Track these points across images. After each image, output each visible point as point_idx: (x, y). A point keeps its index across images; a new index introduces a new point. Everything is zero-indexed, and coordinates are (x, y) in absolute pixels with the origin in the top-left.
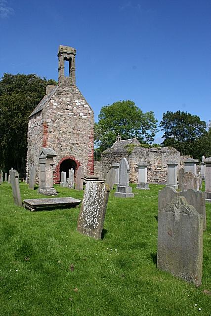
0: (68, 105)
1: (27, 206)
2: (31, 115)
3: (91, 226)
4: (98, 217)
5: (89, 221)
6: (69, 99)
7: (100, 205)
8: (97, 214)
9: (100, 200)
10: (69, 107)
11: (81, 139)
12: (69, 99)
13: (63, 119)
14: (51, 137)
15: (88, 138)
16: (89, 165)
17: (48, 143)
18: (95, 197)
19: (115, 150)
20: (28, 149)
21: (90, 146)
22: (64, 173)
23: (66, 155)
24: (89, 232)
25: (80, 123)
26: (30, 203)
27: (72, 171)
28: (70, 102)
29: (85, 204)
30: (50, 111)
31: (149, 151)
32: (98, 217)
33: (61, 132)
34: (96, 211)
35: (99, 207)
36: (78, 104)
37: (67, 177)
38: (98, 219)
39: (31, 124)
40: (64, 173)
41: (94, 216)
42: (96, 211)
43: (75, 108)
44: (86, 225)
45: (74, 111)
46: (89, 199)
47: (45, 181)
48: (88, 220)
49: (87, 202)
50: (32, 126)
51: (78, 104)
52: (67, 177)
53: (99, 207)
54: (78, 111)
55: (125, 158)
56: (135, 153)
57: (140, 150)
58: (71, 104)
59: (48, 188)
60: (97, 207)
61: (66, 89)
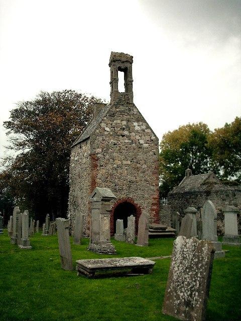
0: (124, 129)
1: (82, 270)
2: (79, 141)
3: (188, 303)
4: (198, 291)
5: (184, 295)
6: (124, 123)
7: (201, 273)
8: (196, 285)
9: (200, 265)
10: (126, 133)
11: (142, 175)
12: (124, 123)
13: (118, 148)
14: (102, 172)
15: (151, 173)
16: (153, 210)
17: (98, 180)
18: (192, 259)
19: (187, 190)
20: (71, 189)
21: (154, 184)
22: (120, 222)
23: (123, 196)
24: (184, 312)
25: (140, 154)
26: (86, 266)
27: (131, 219)
28: (127, 126)
29: (176, 269)
30: (101, 139)
31: (236, 190)
32: (198, 291)
33: (115, 166)
34: (195, 281)
35: (199, 275)
36: (137, 128)
37: (125, 226)
38: (199, 292)
39: (74, 157)
40: (120, 222)
41: (192, 287)
42: (195, 281)
43: (133, 134)
44: (178, 301)
45: (132, 138)
46: (181, 263)
47: (99, 234)
48: (182, 294)
49: (178, 266)
50: (76, 159)
51: (137, 128)
52: (125, 226)
53: (199, 275)
54: (138, 137)
55: (210, 202)
56: (217, 192)
57: (222, 189)
58: (128, 128)
59: (104, 243)
60: (196, 274)
61: (122, 108)
